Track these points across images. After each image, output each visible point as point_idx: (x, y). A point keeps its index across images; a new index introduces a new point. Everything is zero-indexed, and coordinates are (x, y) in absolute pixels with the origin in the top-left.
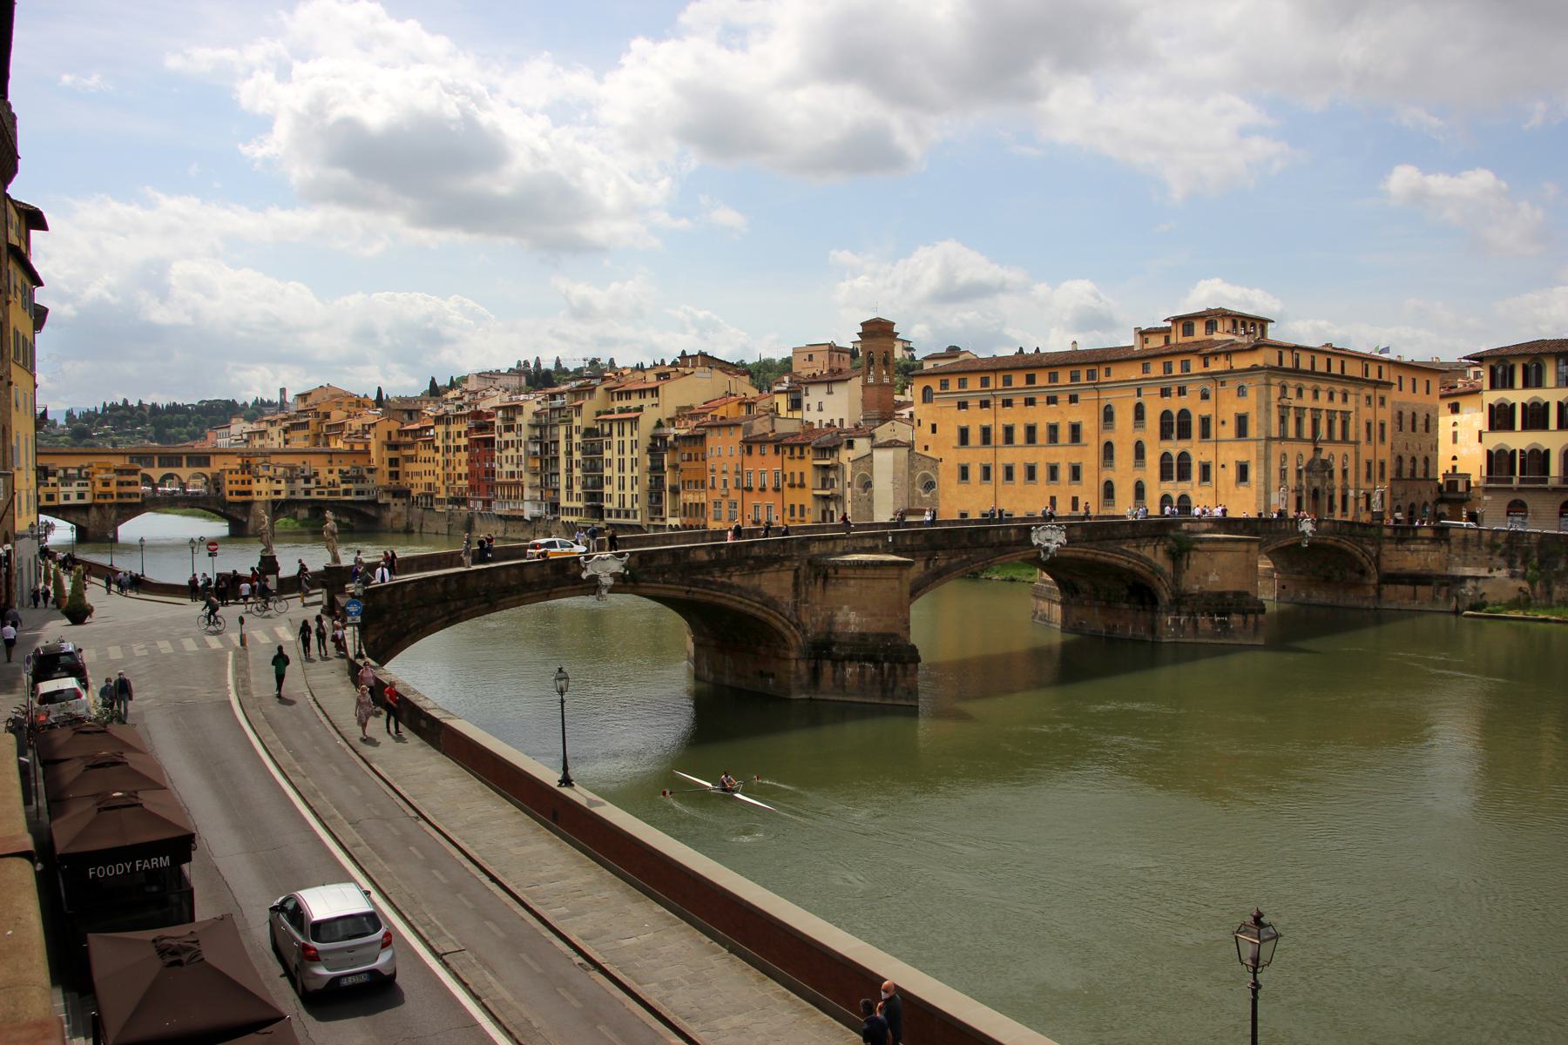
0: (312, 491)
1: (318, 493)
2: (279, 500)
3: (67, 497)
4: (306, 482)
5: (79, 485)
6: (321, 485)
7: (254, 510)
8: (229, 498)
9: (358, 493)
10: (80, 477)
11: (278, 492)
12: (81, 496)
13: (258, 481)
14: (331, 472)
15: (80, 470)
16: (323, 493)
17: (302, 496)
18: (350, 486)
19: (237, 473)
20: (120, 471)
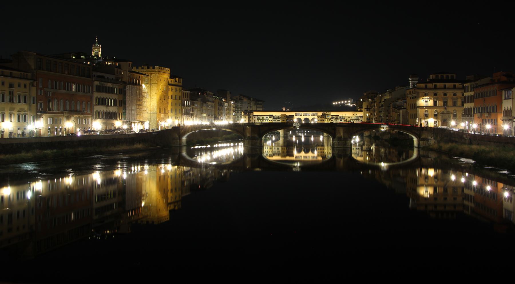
4: (340, 121)
5: (278, 120)
10: (278, 118)
13: (326, 120)
14: (349, 118)
15: (279, 116)
19: (320, 118)
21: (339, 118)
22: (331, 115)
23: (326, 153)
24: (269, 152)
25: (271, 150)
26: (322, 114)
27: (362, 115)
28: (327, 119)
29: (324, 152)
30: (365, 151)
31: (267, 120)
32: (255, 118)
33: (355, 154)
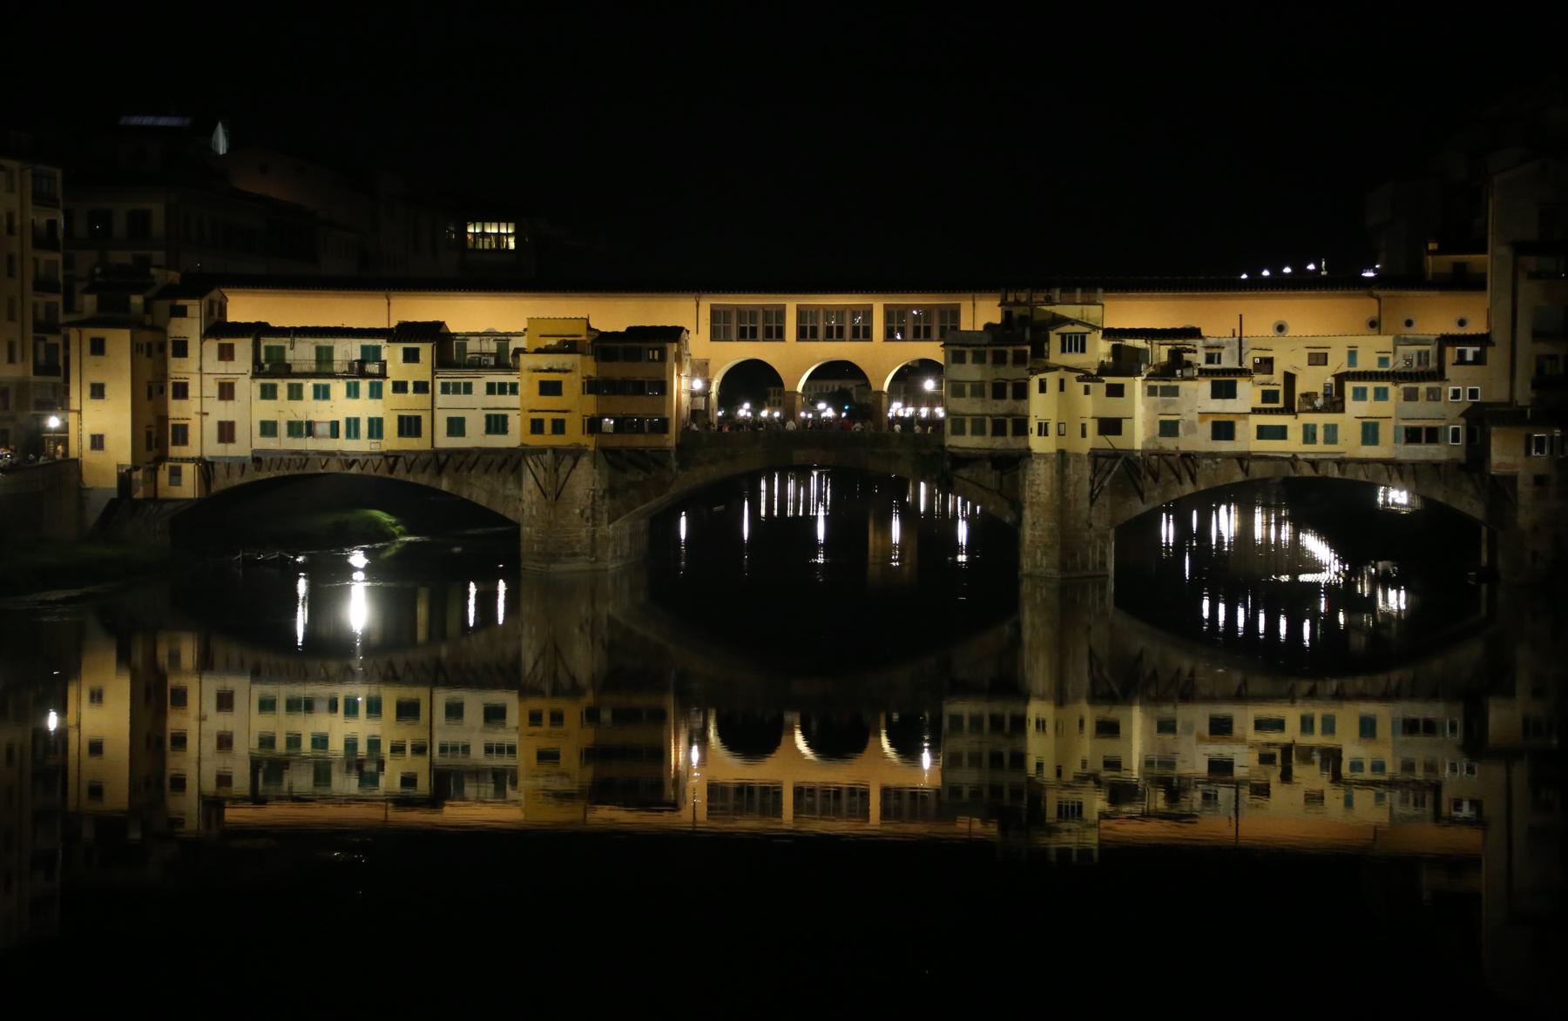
0: (1239, 426)
1: (1263, 433)
2: (1115, 455)
3: (456, 426)
5: (491, 389)
6: (1281, 404)
7: (1032, 483)
8: (952, 441)
9: (1413, 435)
11: (1110, 426)
12: (497, 424)
13: (1043, 388)
14: (1318, 359)
15: (503, 338)
16: (1280, 433)
17: (1199, 440)
18: (1386, 408)
19: (979, 358)
20: (605, 346)
21: (1199, 359)
22: (1106, 326)
23: (1040, 766)
24: (386, 749)
25: (408, 734)
26: (1007, 316)
27: (1476, 327)
28: (1052, 379)
29: (1019, 759)
30: (1507, 755)
31: (364, 385)
32: (226, 354)
33: (1391, 784)
